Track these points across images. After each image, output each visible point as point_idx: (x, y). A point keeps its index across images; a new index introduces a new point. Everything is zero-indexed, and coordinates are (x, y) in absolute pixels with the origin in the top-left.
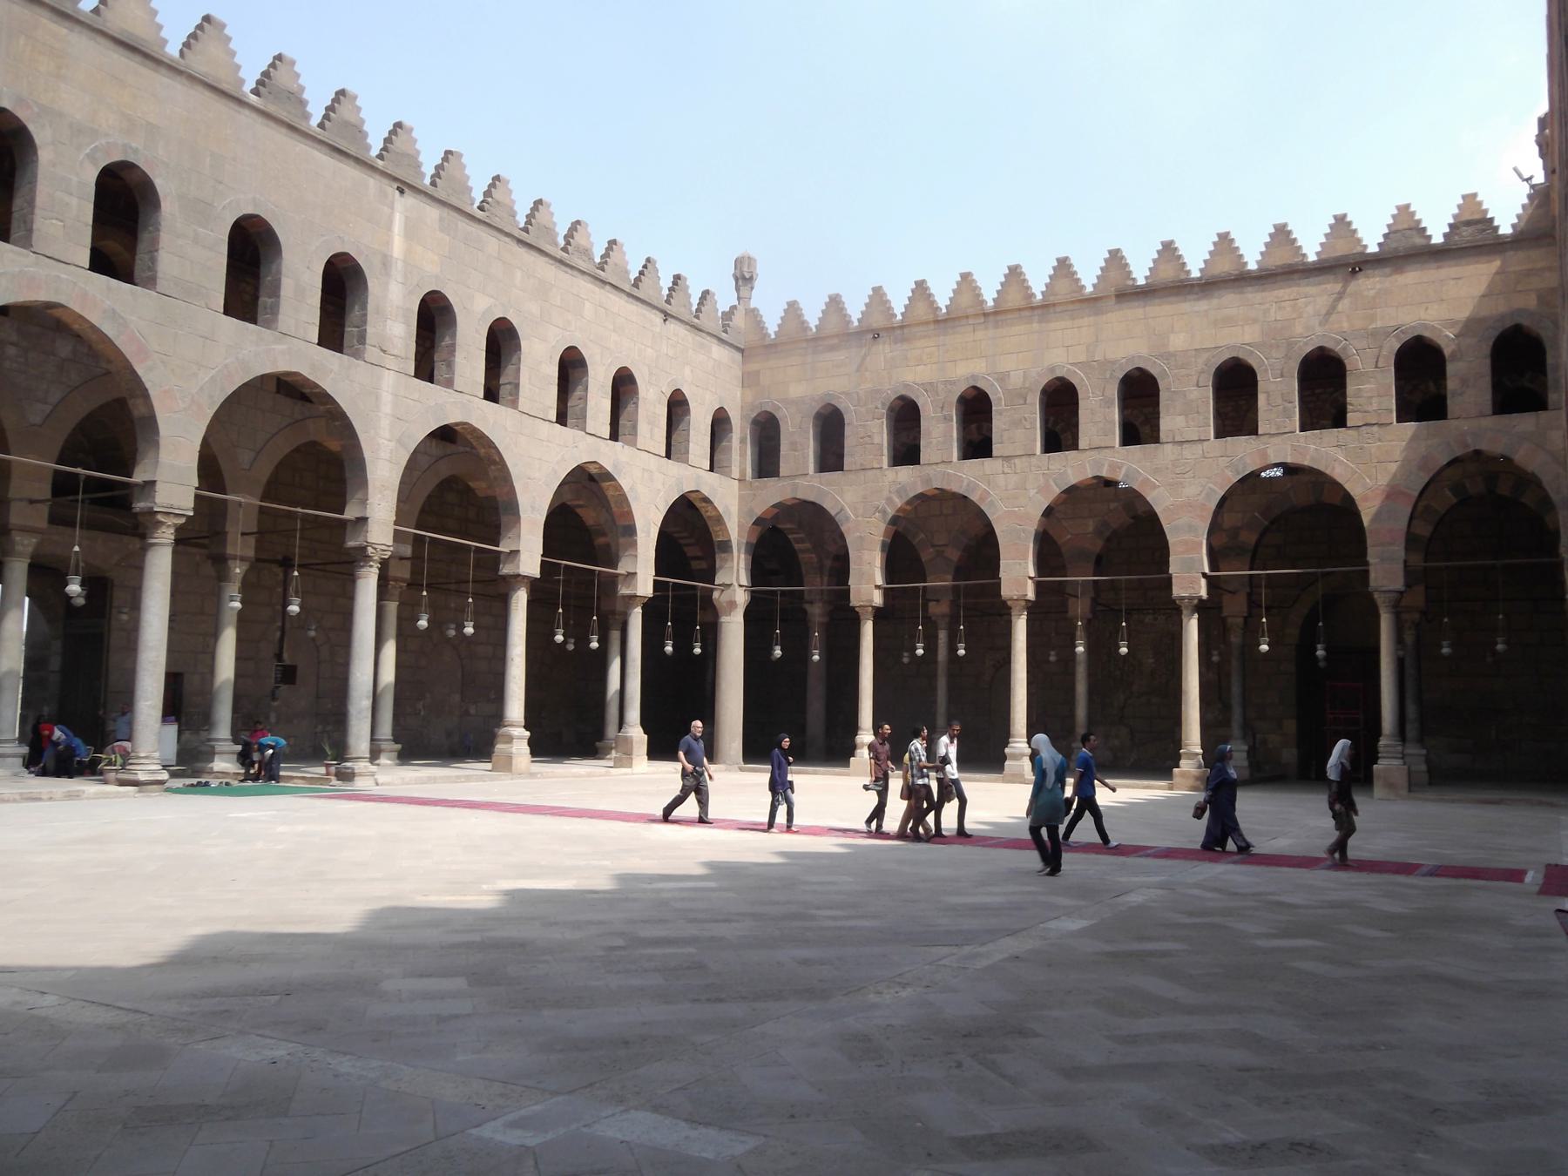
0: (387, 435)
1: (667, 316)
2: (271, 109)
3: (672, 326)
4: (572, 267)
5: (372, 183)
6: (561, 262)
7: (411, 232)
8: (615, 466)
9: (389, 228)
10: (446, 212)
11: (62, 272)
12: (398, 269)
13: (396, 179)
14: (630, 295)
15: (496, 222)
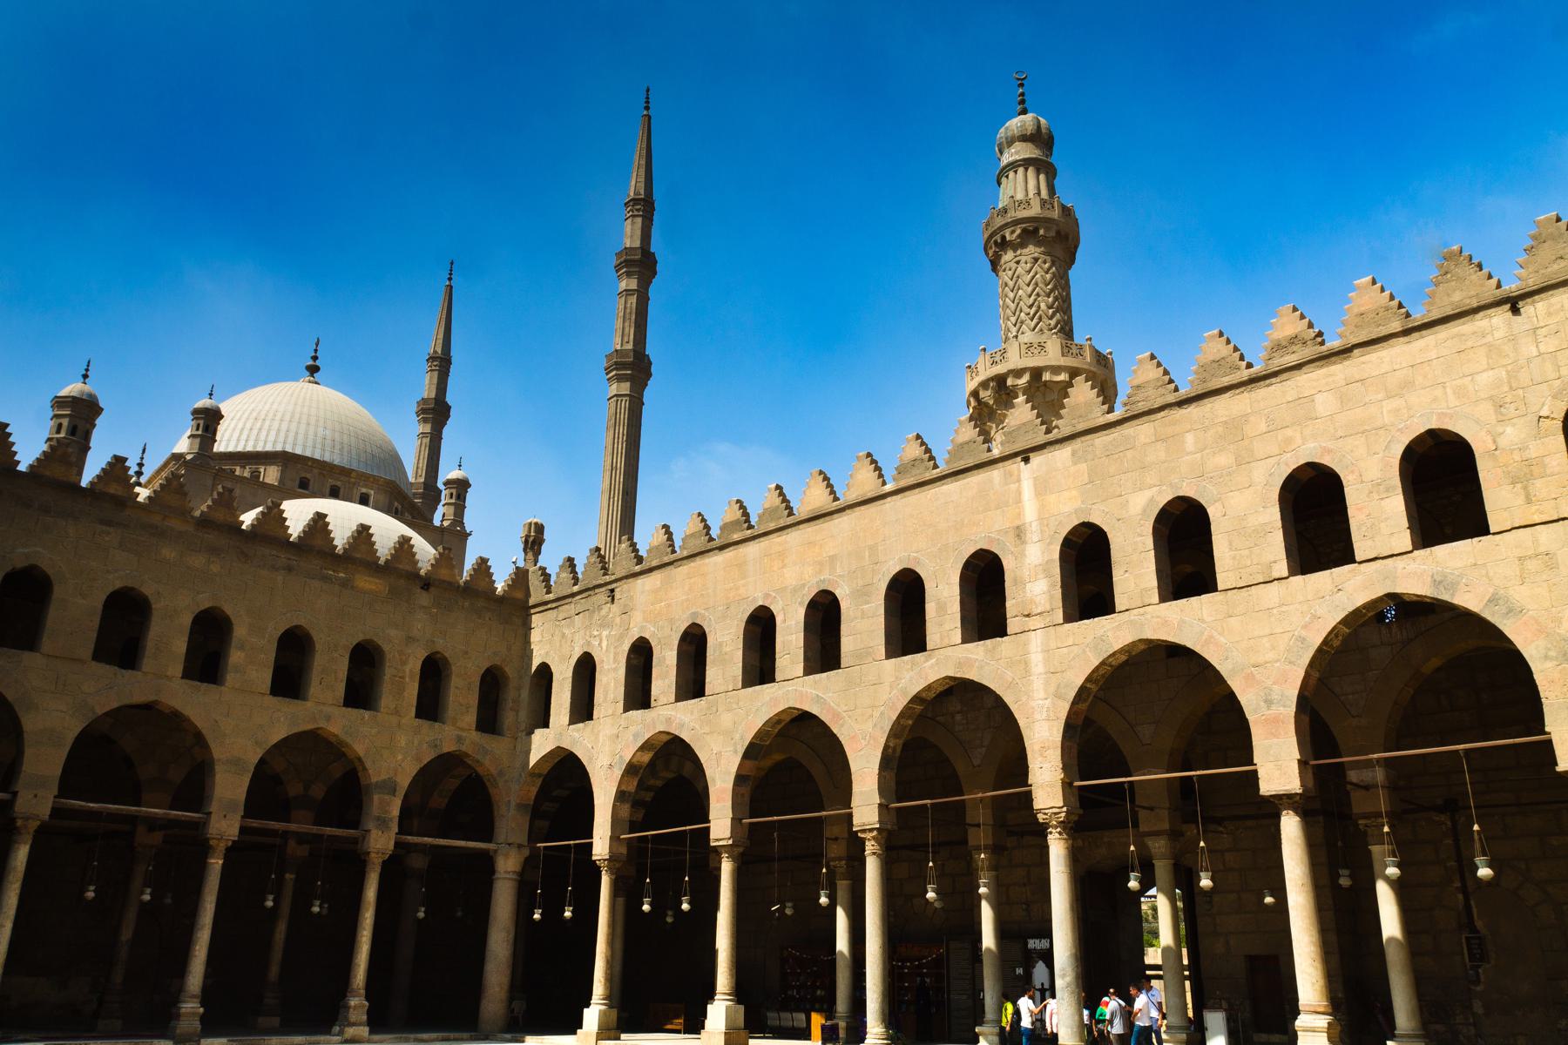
0: (1042, 695)
1: (1513, 304)
2: (903, 483)
3: (1534, 310)
4: (1275, 374)
5: (995, 474)
6: (1254, 380)
7: (1042, 488)
8: (1436, 583)
9: (1019, 500)
10: (1078, 444)
11: (789, 687)
12: (1033, 533)
13: (1015, 455)
14: (1406, 332)
15: (1142, 407)
